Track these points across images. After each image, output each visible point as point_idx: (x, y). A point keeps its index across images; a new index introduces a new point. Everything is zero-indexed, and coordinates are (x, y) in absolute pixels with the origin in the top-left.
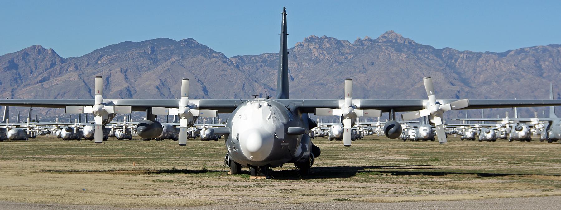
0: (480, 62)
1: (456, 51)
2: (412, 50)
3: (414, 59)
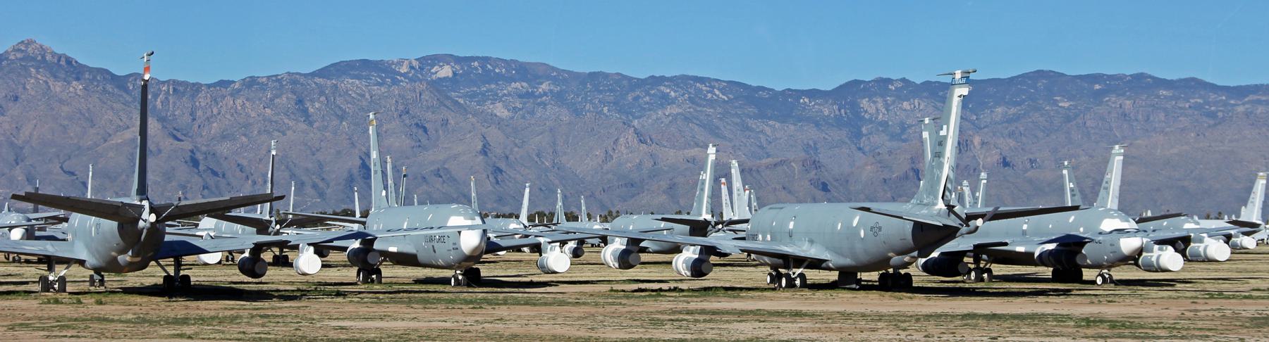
0: (202, 100)
2: (74, 76)
3: (97, 92)
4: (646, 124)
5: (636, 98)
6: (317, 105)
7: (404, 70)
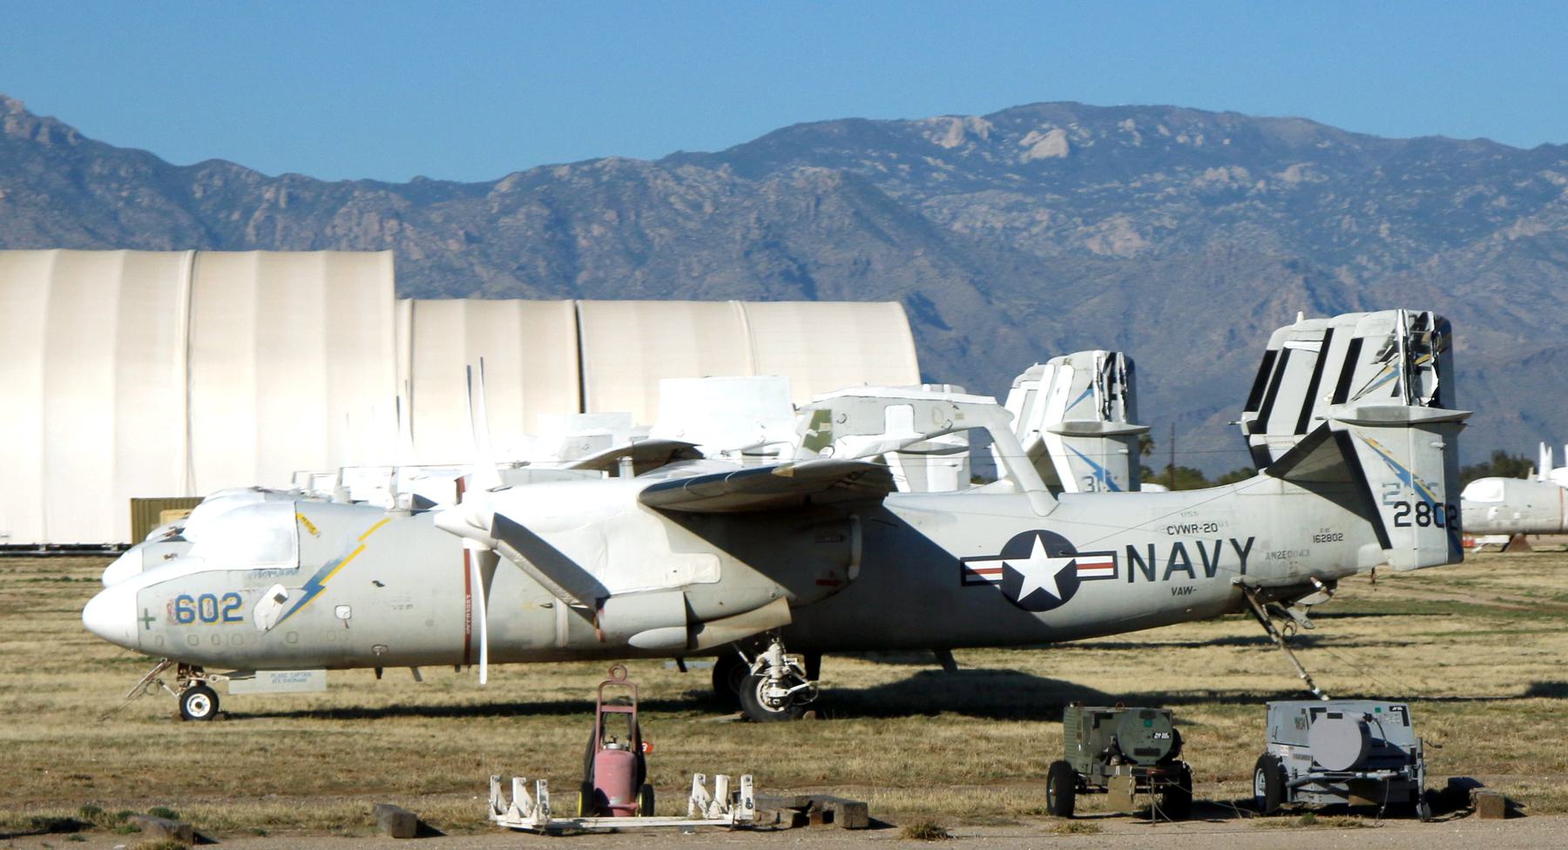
1: (250, 173)
3: (36, 205)
4: (1458, 264)
5: (1475, 202)
6: (597, 230)
7: (951, 141)
